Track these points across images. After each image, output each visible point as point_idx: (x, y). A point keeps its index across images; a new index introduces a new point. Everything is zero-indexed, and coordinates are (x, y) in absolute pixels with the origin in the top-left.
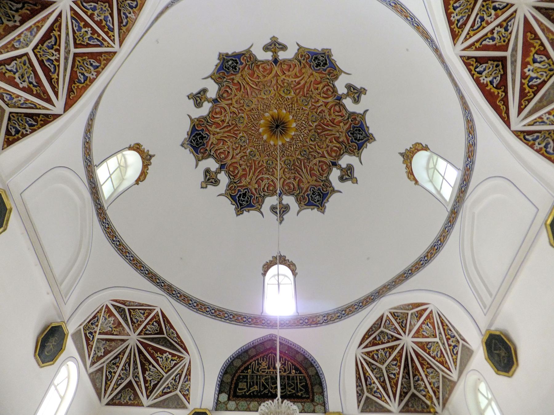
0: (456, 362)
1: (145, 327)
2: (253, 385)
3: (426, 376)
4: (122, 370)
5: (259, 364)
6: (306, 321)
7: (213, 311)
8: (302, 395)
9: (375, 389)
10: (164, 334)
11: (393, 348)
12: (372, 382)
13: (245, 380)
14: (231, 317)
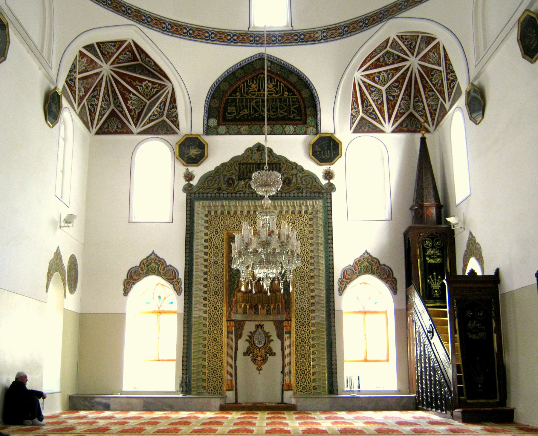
0: (451, 95)
1: (117, 57)
2: (243, 109)
3: (427, 98)
4: (103, 101)
5: (248, 86)
6: (302, 37)
7: (191, 32)
8: (294, 117)
9: (371, 111)
10: (138, 61)
11: (397, 69)
12: (369, 104)
13: (234, 104)
14: (213, 36)
